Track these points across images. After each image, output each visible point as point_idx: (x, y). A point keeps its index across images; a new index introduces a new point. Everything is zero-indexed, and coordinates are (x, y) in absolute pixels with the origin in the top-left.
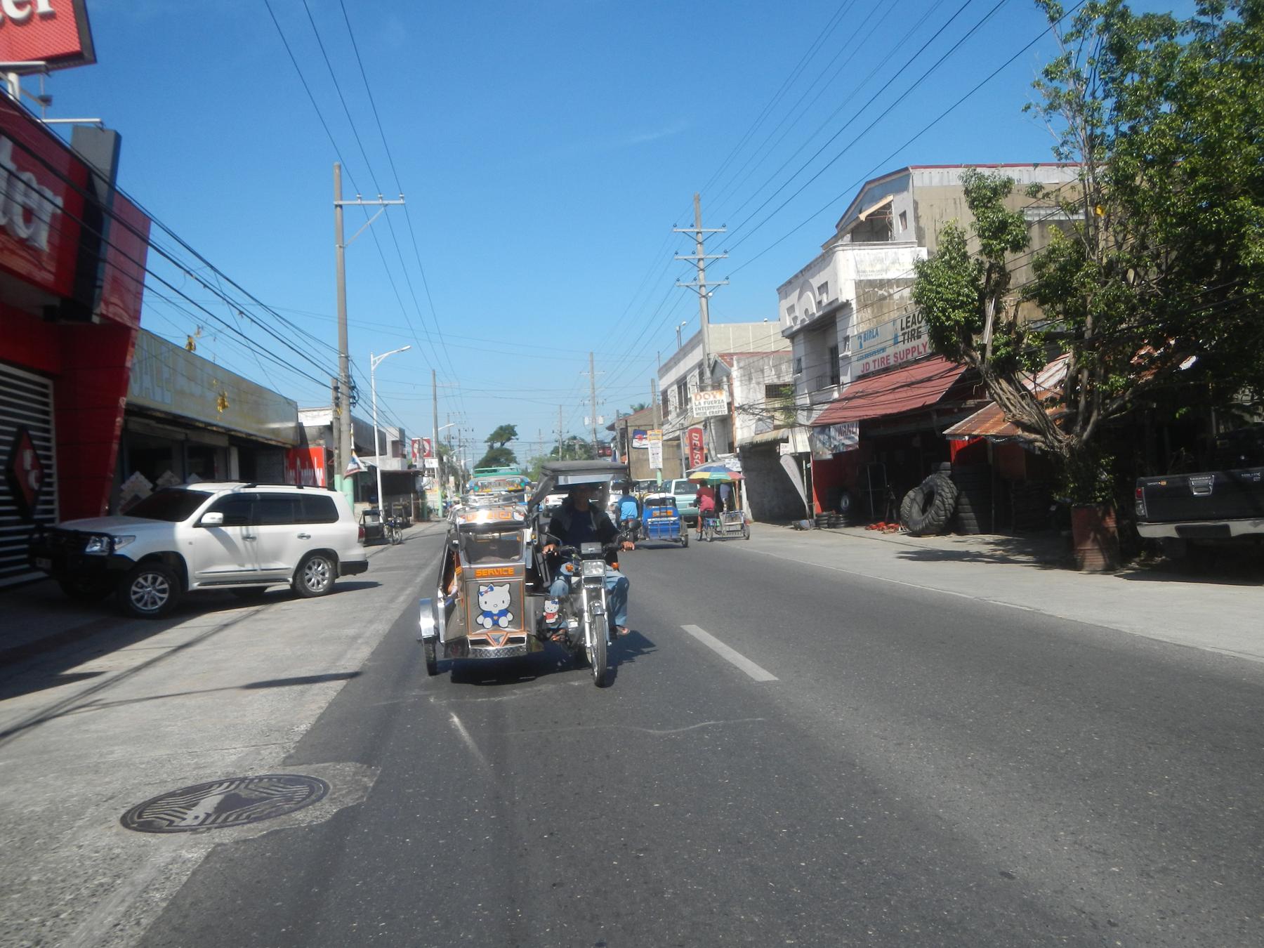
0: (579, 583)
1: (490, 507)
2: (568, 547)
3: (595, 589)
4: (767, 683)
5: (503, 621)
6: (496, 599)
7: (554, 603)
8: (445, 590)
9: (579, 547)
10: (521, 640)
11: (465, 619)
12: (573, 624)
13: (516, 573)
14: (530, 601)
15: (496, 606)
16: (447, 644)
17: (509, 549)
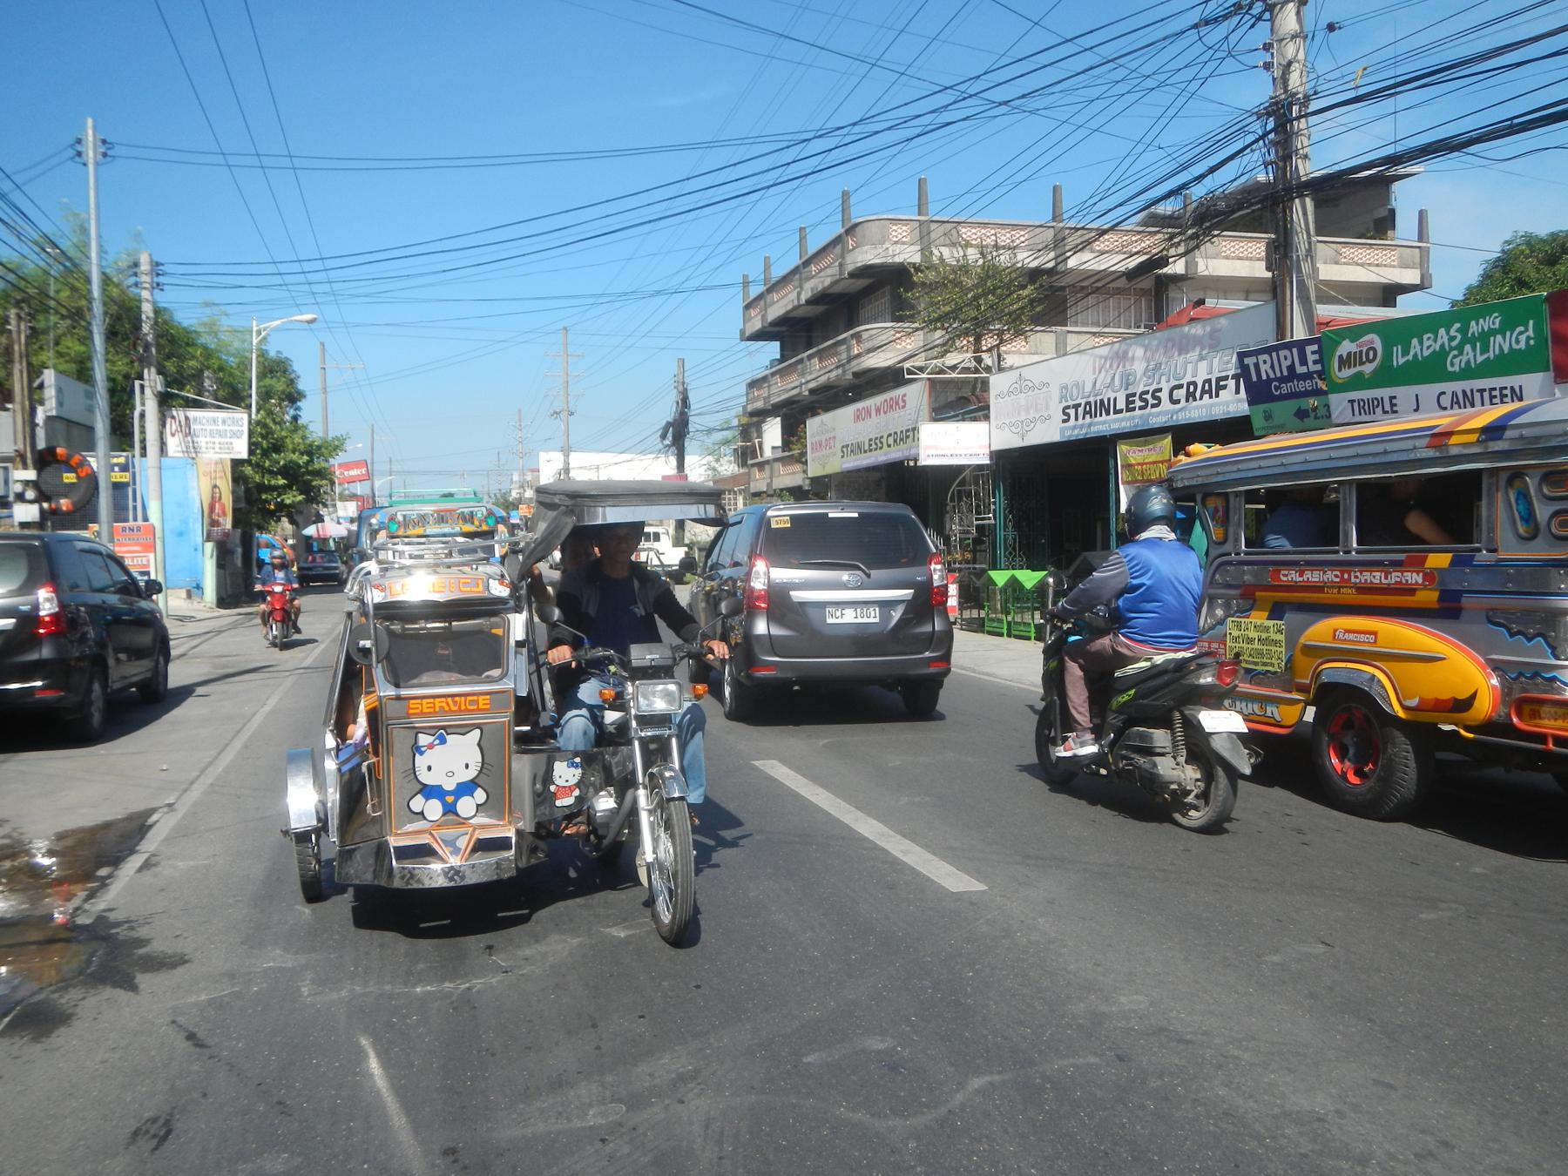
0: (623, 727)
1: (434, 567)
2: (600, 652)
3: (654, 739)
4: (958, 897)
5: (466, 806)
6: (451, 760)
8: (341, 732)
9: (624, 651)
10: (501, 844)
12: (605, 803)
14: (523, 766)
17: (479, 654)
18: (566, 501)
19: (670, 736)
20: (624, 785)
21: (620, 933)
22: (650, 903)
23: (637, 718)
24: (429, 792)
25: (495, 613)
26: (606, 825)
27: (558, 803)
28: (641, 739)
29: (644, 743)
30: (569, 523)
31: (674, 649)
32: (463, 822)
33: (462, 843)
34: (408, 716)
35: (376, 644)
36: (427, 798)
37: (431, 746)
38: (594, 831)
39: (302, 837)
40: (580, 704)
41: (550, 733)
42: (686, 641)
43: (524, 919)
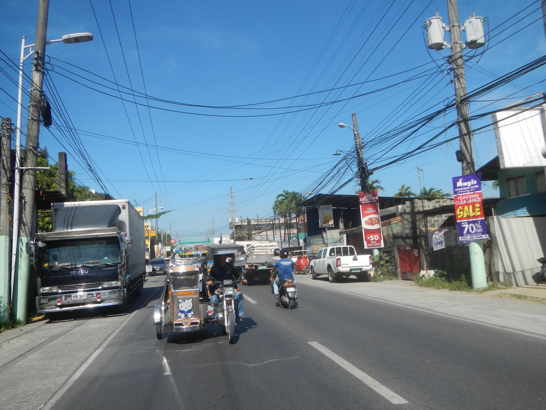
0: (223, 297)
1: (185, 265)
2: (218, 282)
3: (229, 300)
5: (189, 315)
6: (186, 305)
8: (165, 301)
9: (222, 282)
10: (197, 323)
11: (172, 314)
12: (220, 316)
13: (195, 293)
14: (201, 306)
15: (186, 308)
16: (165, 326)
21: (220, 343)
24: (182, 312)
25: (196, 274)
28: (226, 300)
40: (215, 294)
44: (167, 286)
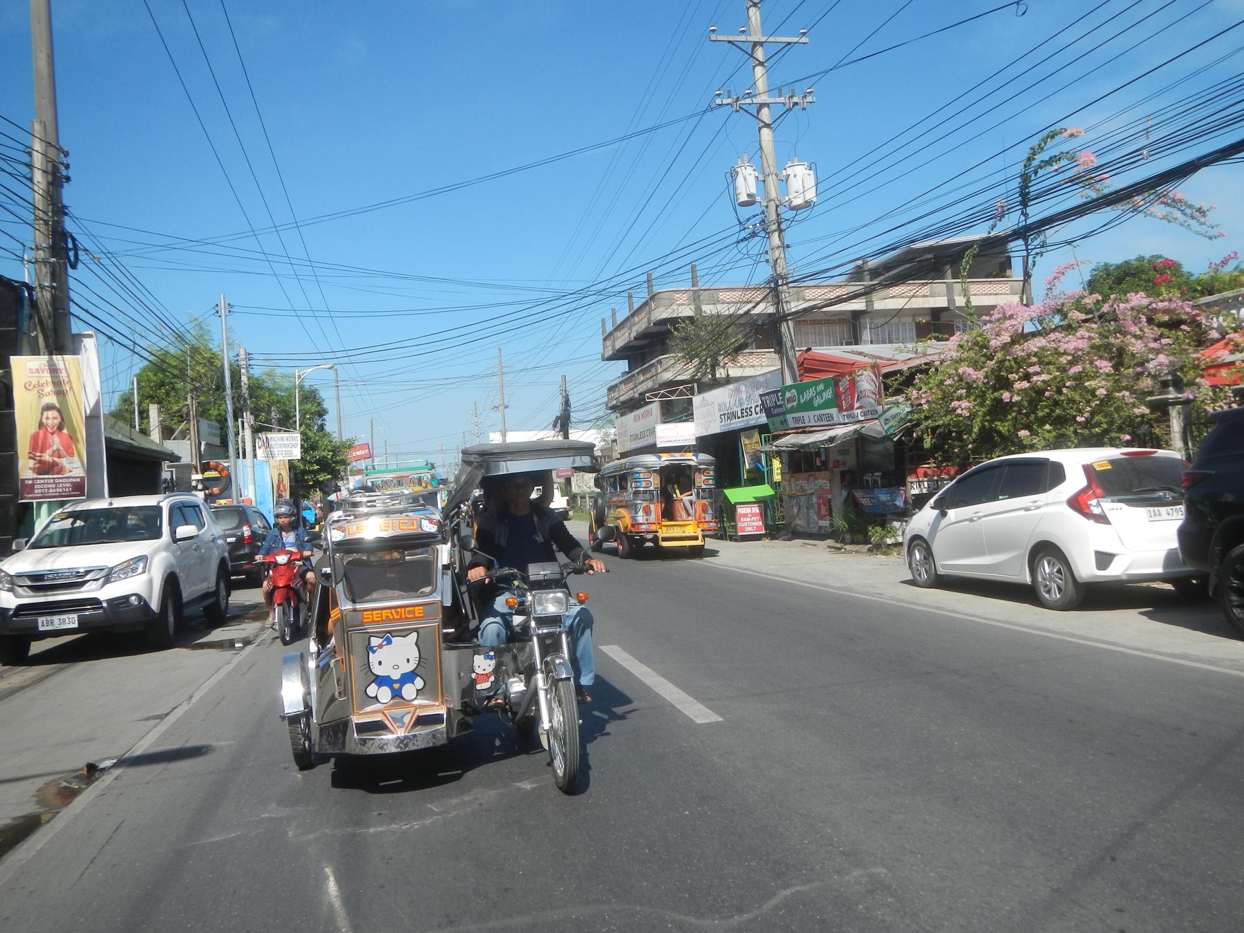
0: (525, 627)
2: (506, 571)
5: (409, 691)
6: (398, 656)
7: (488, 657)
9: (524, 569)
10: (436, 719)
14: (451, 658)
15: (396, 667)
18: (479, 460)
19: (560, 633)
20: (528, 672)
21: (527, 786)
22: (550, 764)
23: (536, 619)
24: (382, 681)
25: (428, 545)
26: (518, 704)
27: (478, 687)
28: (538, 636)
29: (542, 639)
30: (480, 475)
31: (566, 566)
32: (407, 703)
33: (407, 719)
34: (362, 624)
35: (334, 569)
36: (379, 686)
37: (380, 646)
38: (511, 710)
39: (294, 720)
40: (495, 614)
41: (475, 633)
42: (573, 560)
43: (457, 777)
44: (325, 590)
